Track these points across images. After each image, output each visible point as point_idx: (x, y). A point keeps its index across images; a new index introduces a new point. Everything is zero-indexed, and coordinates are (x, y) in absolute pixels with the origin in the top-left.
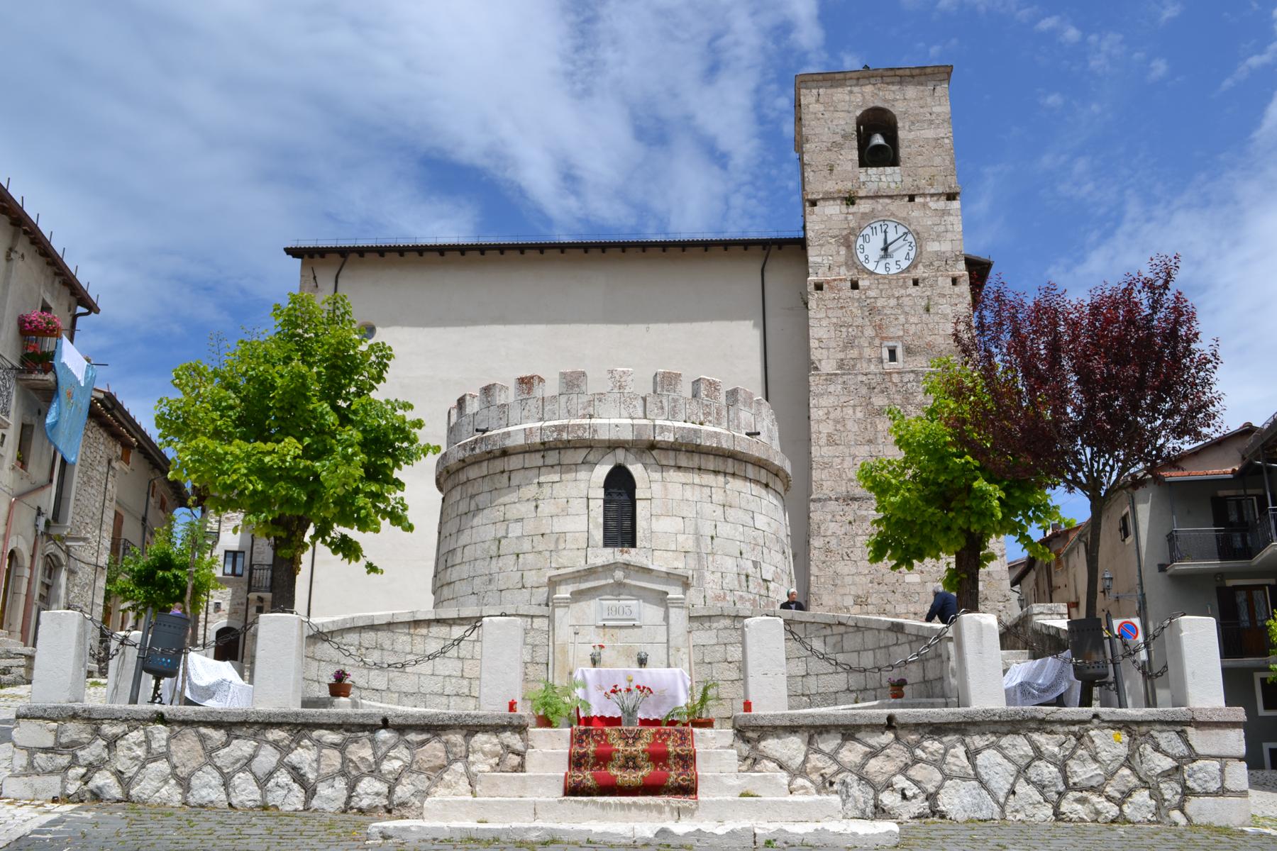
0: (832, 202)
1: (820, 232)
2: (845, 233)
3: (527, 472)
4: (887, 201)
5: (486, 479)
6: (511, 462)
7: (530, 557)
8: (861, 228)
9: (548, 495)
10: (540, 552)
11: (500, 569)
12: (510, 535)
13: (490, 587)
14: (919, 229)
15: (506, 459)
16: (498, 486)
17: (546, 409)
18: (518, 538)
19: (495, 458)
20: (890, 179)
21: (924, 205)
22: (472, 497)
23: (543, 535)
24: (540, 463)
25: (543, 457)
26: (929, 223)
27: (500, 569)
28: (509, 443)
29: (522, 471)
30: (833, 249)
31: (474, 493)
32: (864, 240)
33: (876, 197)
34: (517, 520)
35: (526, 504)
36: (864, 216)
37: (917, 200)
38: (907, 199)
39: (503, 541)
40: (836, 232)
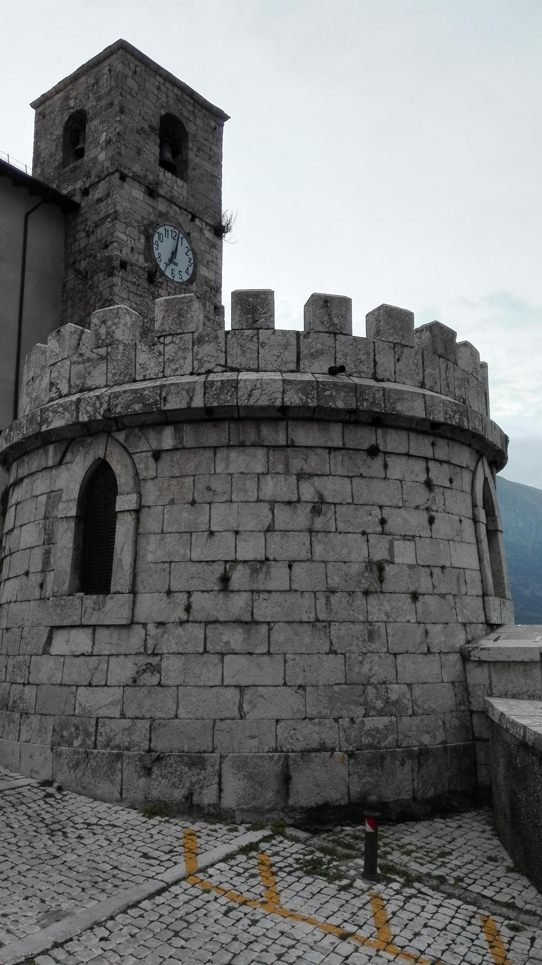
0: (138, 185)
1: (127, 210)
2: (146, 222)
3: (411, 462)
4: (177, 209)
5: (339, 455)
6: (389, 438)
7: (432, 602)
8: (158, 225)
9: (441, 507)
10: (443, 596)
11: (387, 615)
12: (397, 560)
13: (374, 646)
14: (196, 248)
15: (380, 432)
16: (364, 471)
17: (427, 372)
18: (410, 566)
19: (357, 423)
20: (179, 190)
21: (201, 230)
22: (301, 476)
23: (443, 568)
24: (430, 455)
25: (433, 444)
26: (203, 248)
27: (387, 615)
28: (402, 408)
29: (404, 459)
30: (136, 231)
31: (307, 469)
32: (159, 239)
33: (171, 201)
34: (405, 538)
35: (415, 513)
36: (161, 215)
37: (197, 221)
38: (190, 217)
39: (388, 568)
40: (139, 218)
